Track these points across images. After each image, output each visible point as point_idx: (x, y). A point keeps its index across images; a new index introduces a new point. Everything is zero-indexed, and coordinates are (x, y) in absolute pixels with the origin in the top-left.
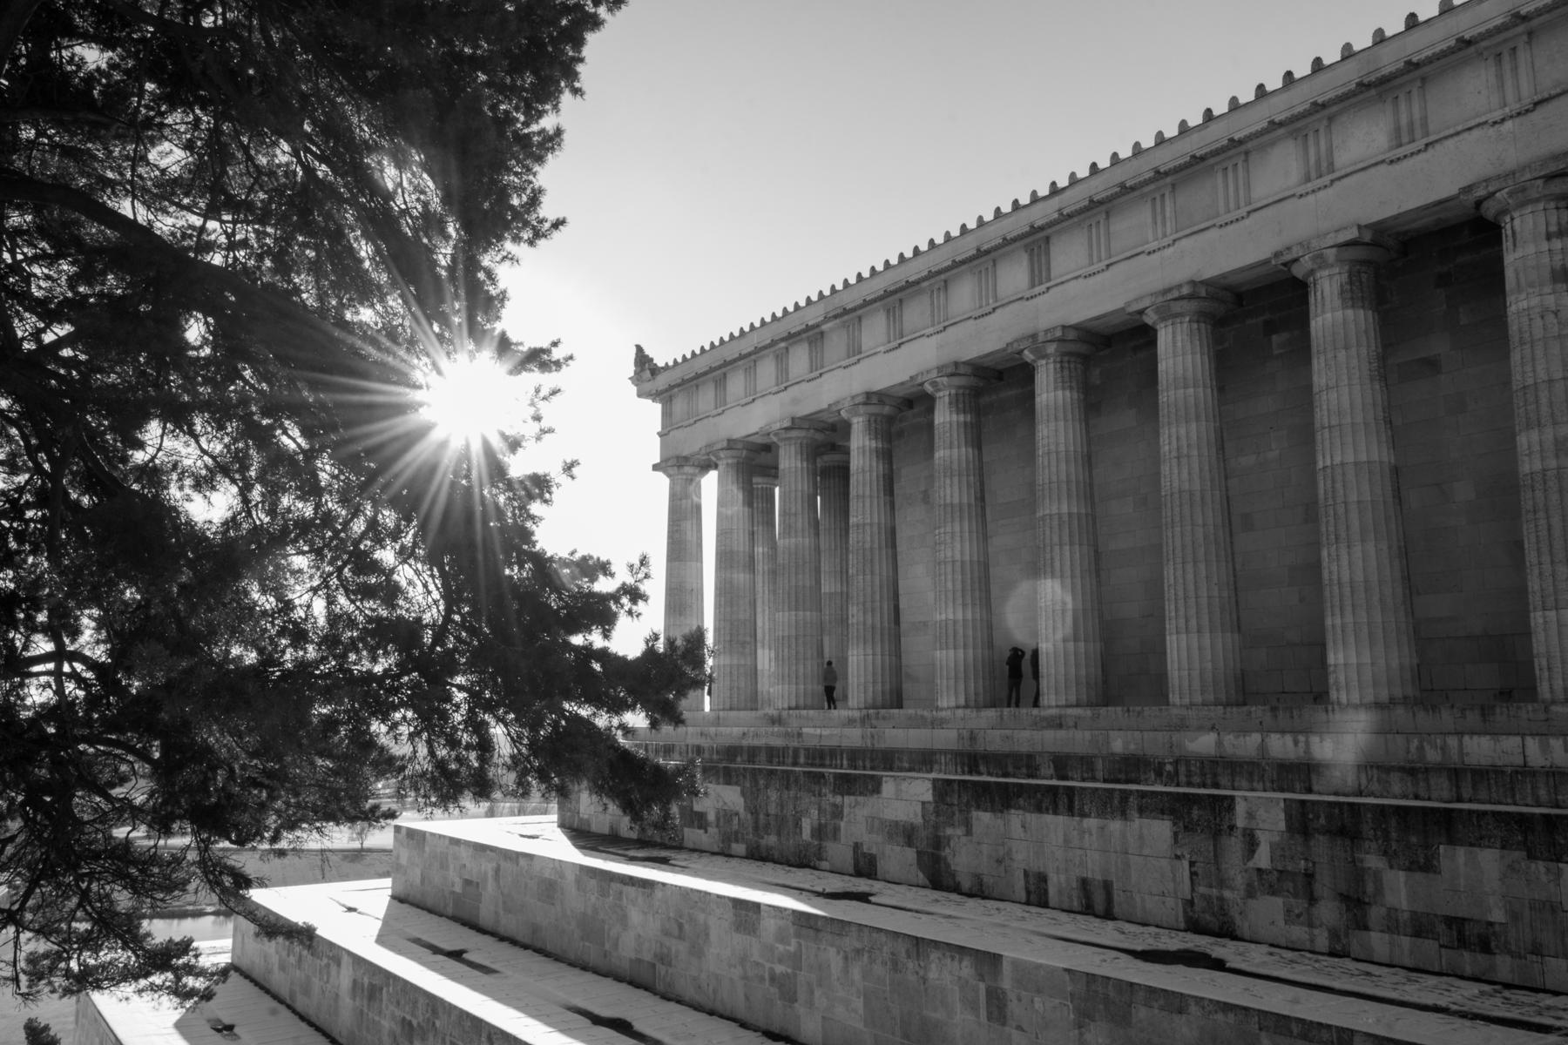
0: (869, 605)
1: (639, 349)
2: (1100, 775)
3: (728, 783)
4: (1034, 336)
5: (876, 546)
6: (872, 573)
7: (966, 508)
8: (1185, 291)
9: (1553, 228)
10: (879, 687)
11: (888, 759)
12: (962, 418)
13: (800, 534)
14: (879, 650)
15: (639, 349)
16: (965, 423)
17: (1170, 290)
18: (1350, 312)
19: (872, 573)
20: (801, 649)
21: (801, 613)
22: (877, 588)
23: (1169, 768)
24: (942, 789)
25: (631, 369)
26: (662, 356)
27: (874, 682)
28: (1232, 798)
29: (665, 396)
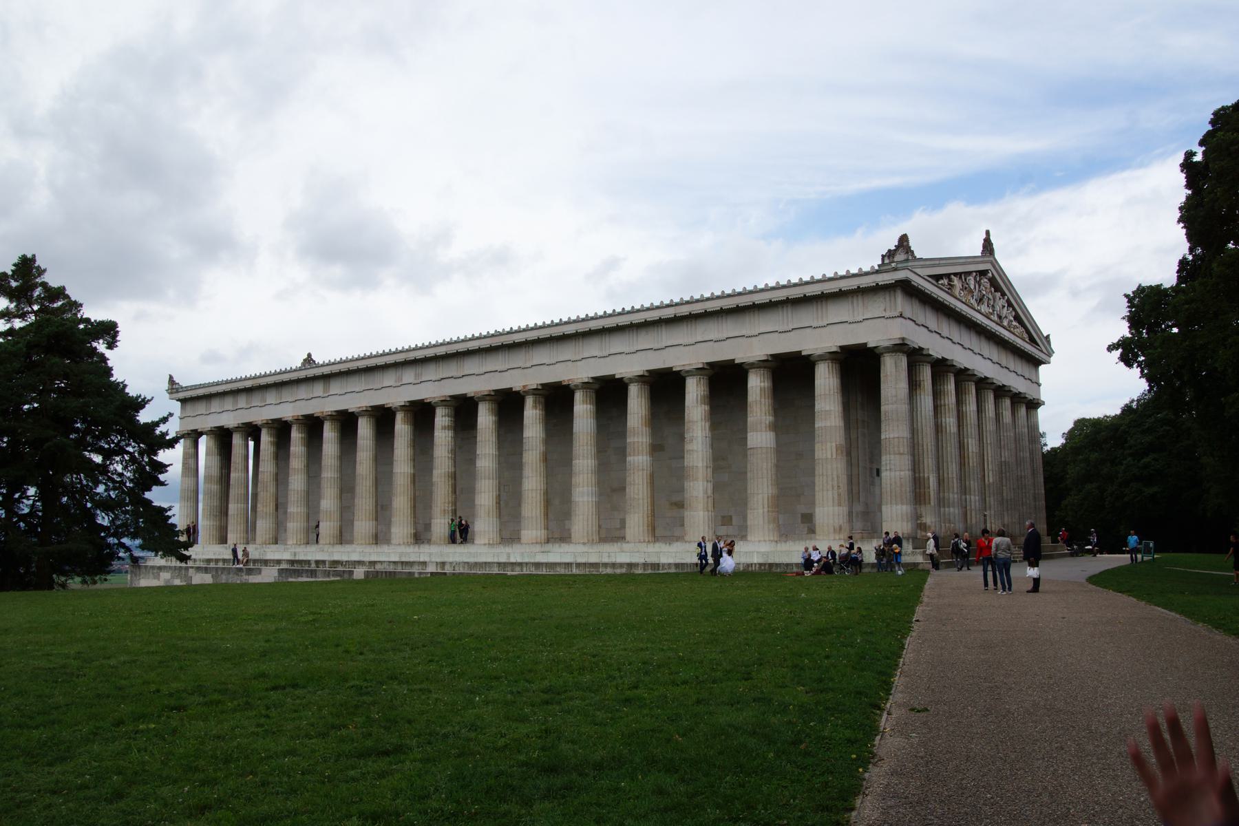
0: (265, 504)
1: (171, 377)
2: (327, 566)
3: (207, 573)
4: (323, 412)
5: (269, 480)
6: (267, 491)
7: (300, 470)
8: (364, 409)
9: (444, 414)
10: (268, 536)
11: (266, 562)
12: (300, 435)
13: (240, 471)
14: (268, 522)
15: (171, 377)
16: (302, 438)
17: (360, 407)
18: (403, 426)
19: (267, 491)
20: (239, 520)
21: (239, 505)
22: (268, 497)
23: (344, 563)
24: (281, 571)
25: (166, 386)
26: (183, 381)
27: (266, 534)
28: (353, 571)
29: (184, 401)
